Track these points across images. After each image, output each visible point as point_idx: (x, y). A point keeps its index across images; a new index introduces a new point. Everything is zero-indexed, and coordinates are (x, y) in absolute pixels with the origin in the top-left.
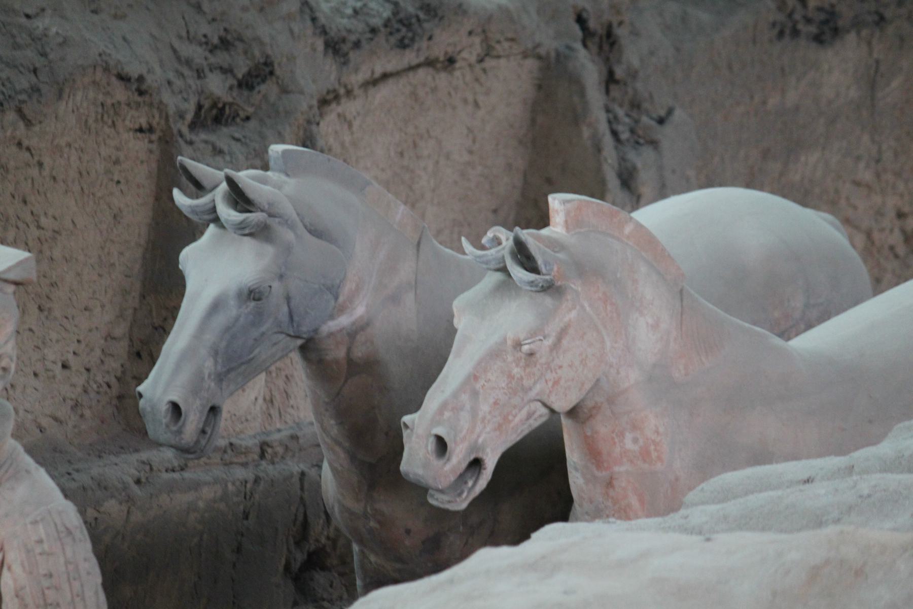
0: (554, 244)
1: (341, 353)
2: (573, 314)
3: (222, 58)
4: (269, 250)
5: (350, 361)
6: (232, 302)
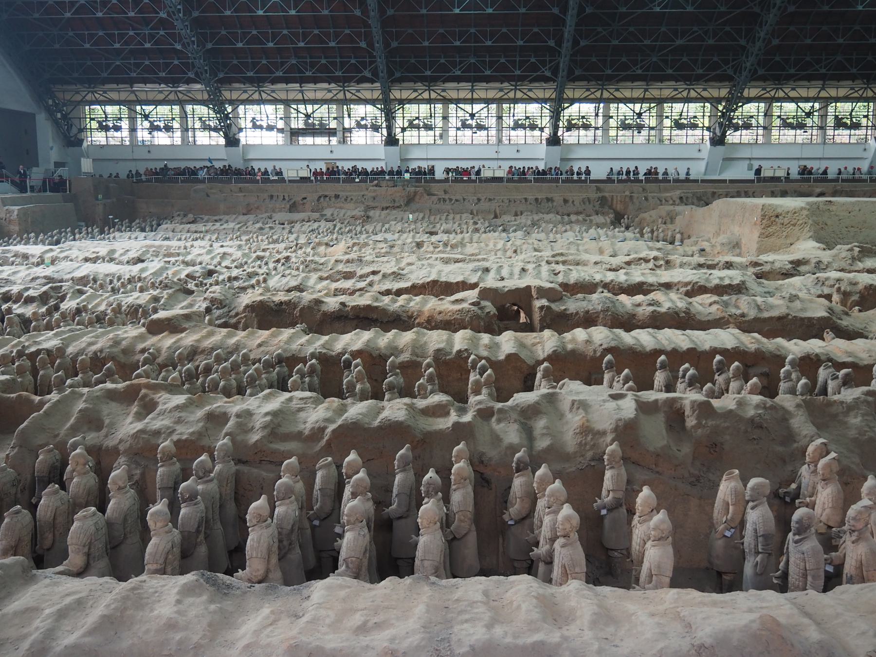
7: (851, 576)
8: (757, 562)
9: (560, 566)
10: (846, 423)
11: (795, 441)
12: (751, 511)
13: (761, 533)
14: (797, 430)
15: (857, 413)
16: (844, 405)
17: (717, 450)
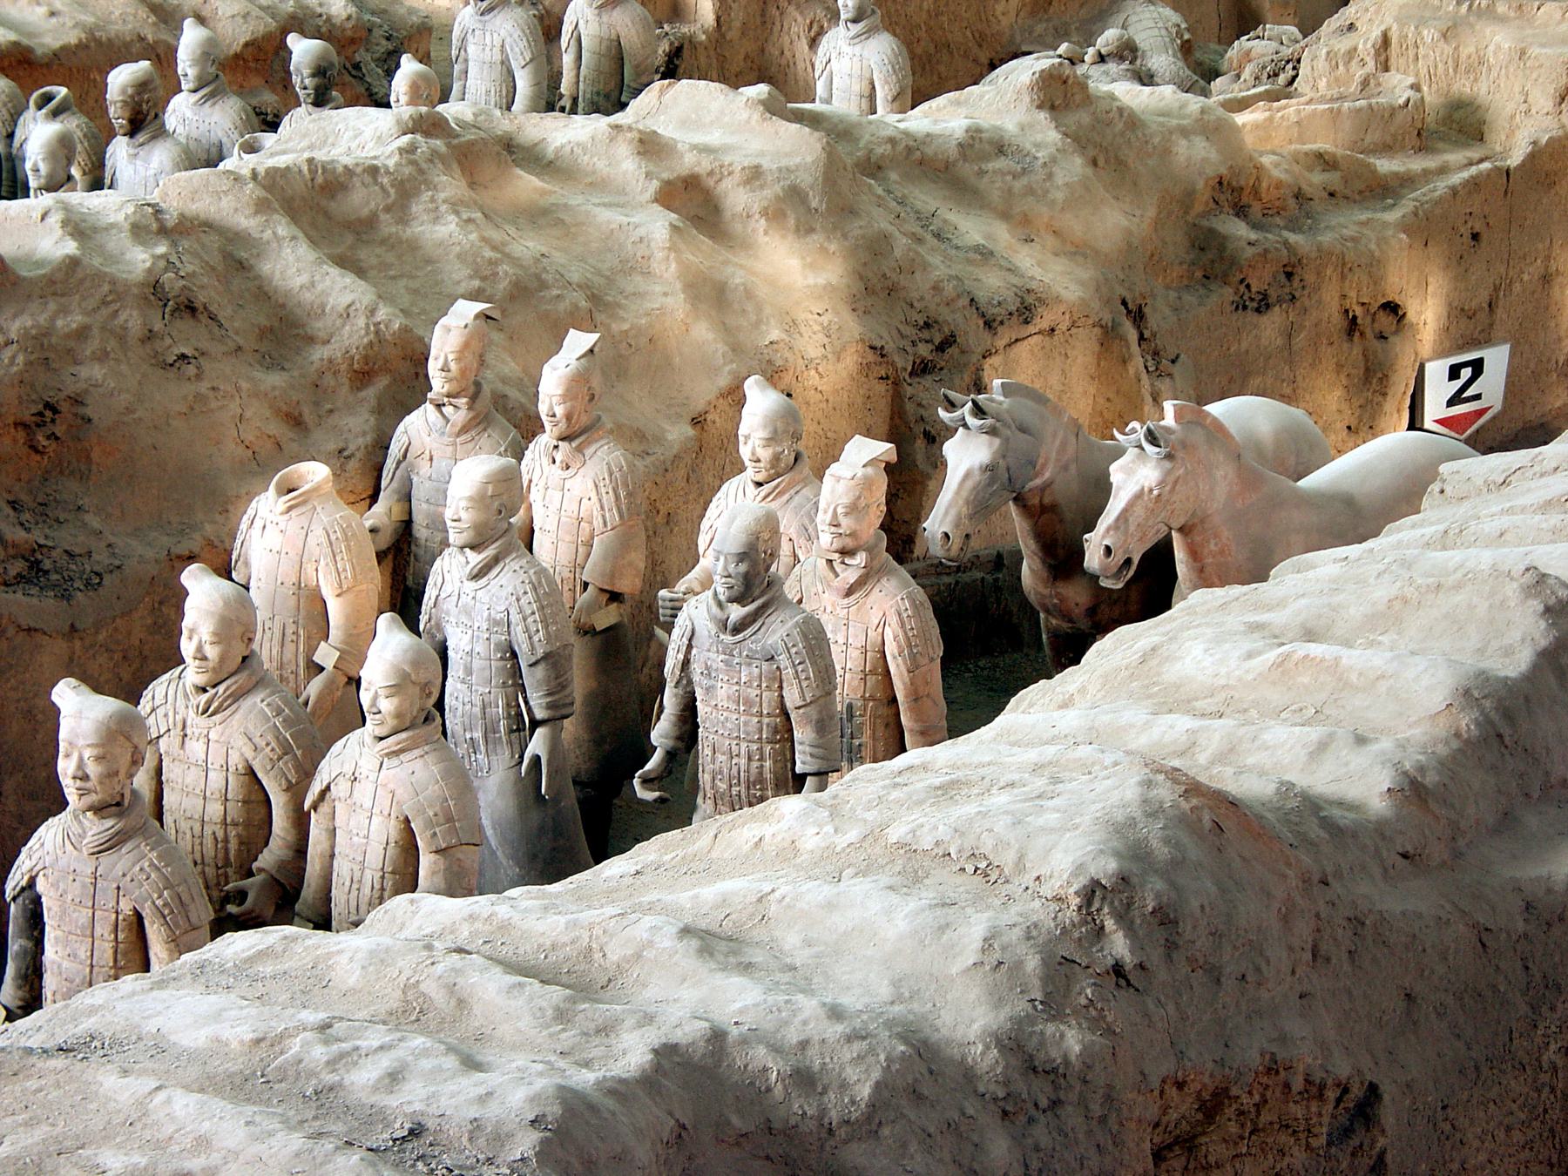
0: (1167, 430)
1: (1036, 501)
2: (1181, 471)
3: (926, 334)
4: (997, 441)
5: (1041, 505)
6: (977, 473)
7: (850, 706)
8: (536, 760)
9: (103, 930)
10: (413, 246)
11: (311, 340)
12: (471, 586)
13: (540, 652)
14: (308, 296)
15: (433, 200)
16: (385, 180)
17: (59, 430)
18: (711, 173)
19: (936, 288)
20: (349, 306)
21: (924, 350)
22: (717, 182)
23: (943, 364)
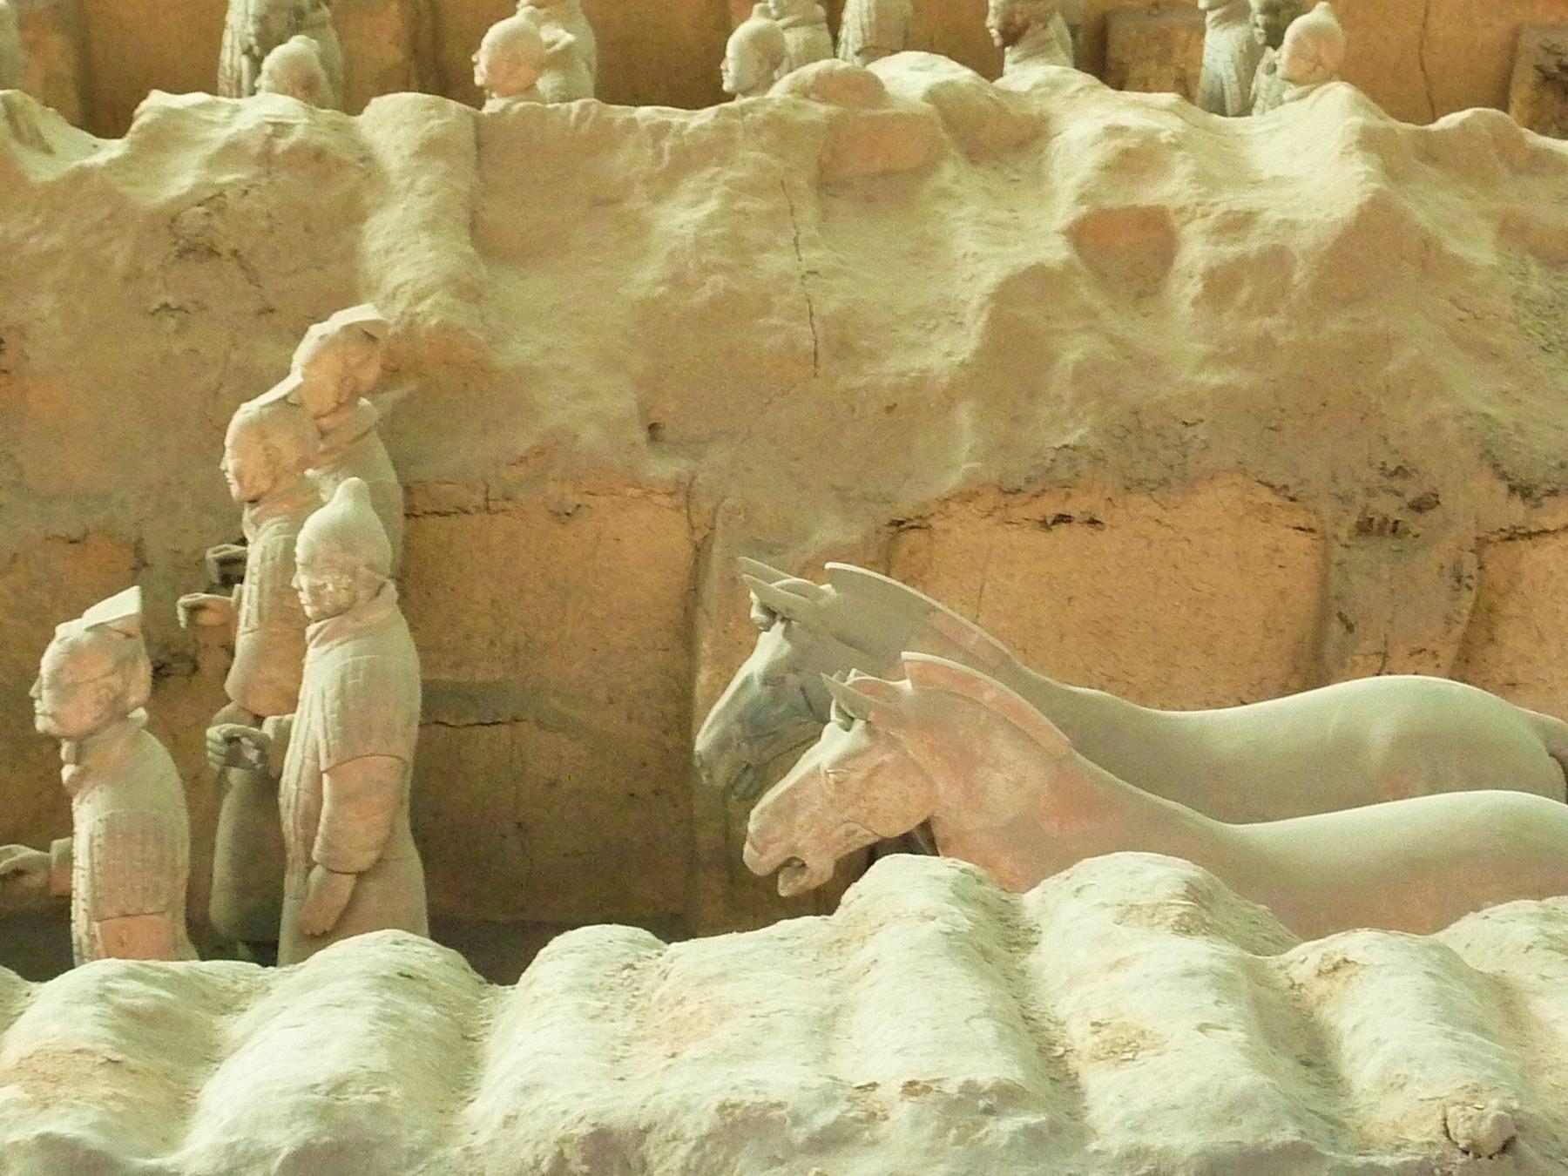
2: (887, 758)
4: (787, 647)
6: (757, 683)
15: (713, 179)
18: (1182, 210)
19: (1433, 426)
20: (400, 286)
21: (1387, 507)
22: (1185, 224)
23: (1419, 530)
